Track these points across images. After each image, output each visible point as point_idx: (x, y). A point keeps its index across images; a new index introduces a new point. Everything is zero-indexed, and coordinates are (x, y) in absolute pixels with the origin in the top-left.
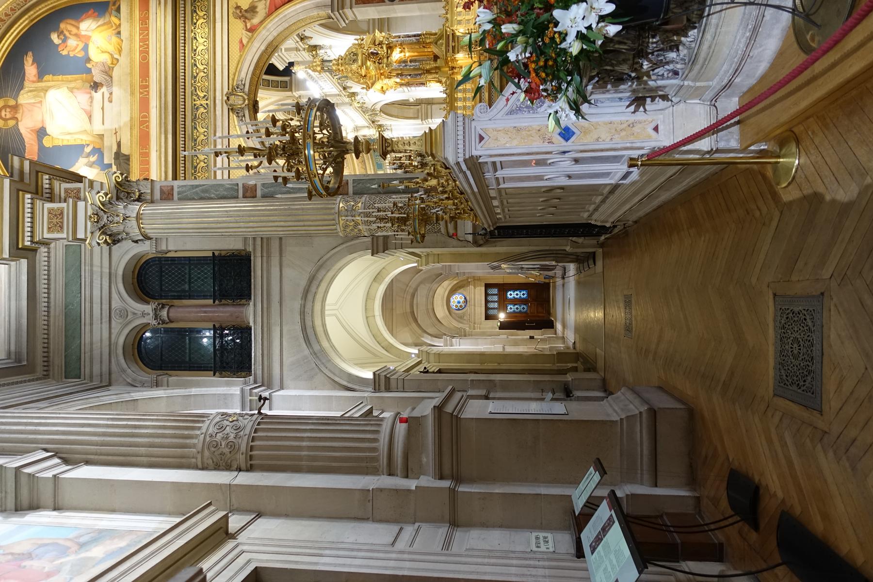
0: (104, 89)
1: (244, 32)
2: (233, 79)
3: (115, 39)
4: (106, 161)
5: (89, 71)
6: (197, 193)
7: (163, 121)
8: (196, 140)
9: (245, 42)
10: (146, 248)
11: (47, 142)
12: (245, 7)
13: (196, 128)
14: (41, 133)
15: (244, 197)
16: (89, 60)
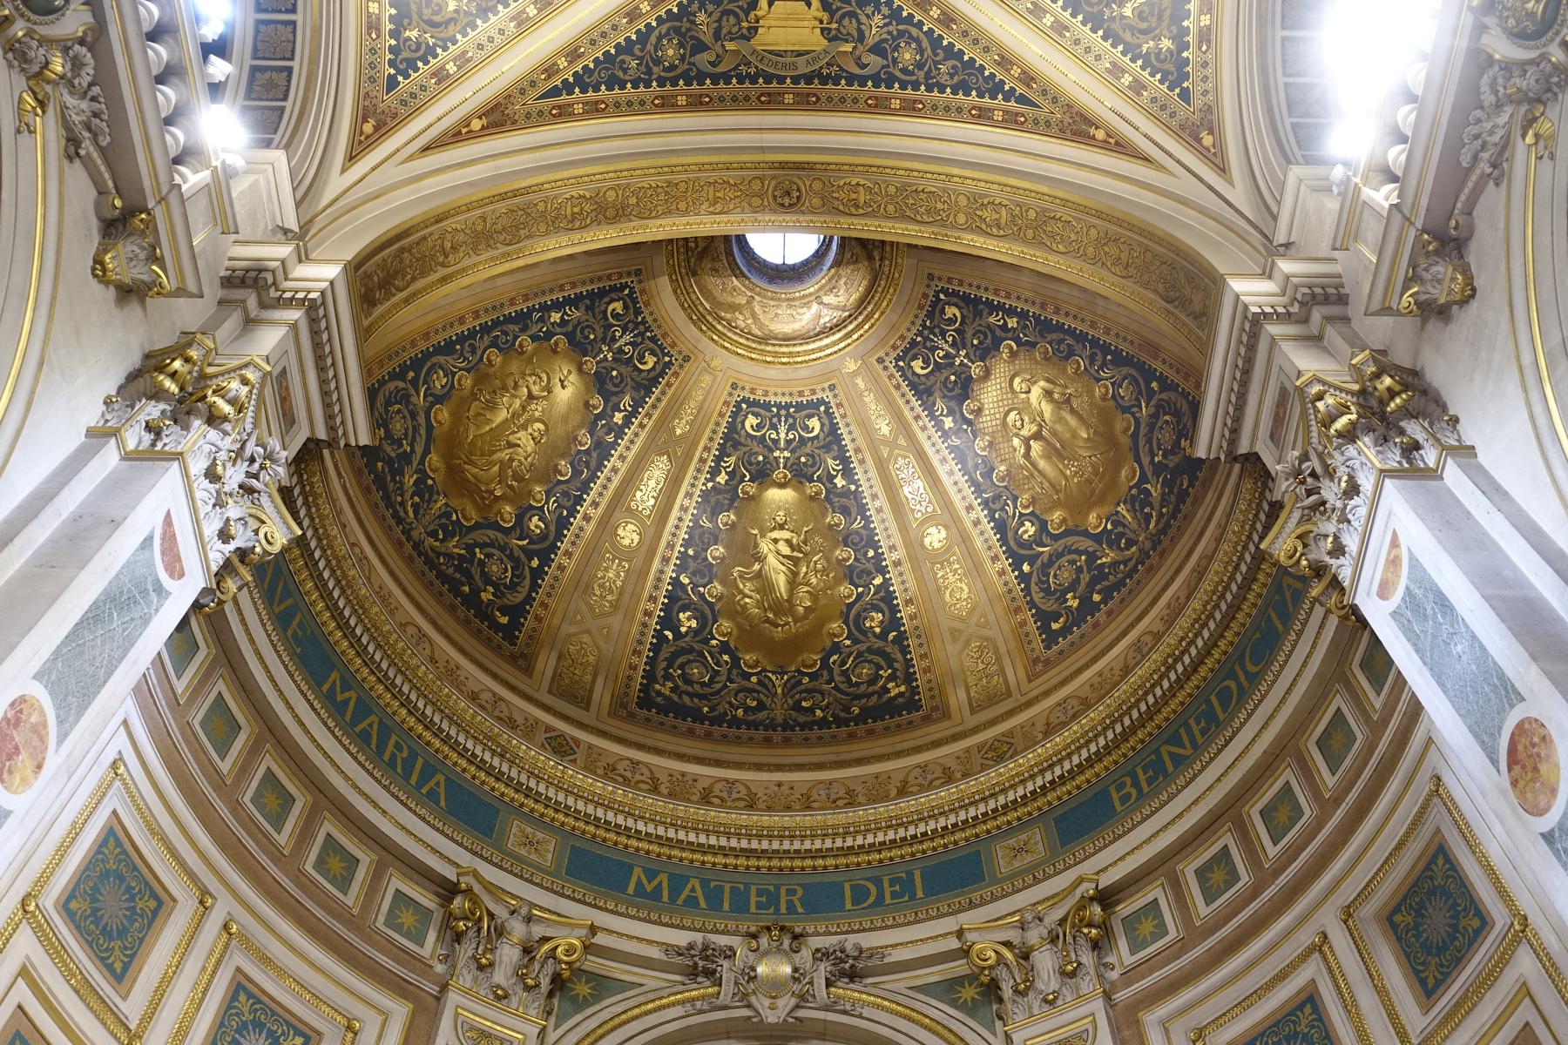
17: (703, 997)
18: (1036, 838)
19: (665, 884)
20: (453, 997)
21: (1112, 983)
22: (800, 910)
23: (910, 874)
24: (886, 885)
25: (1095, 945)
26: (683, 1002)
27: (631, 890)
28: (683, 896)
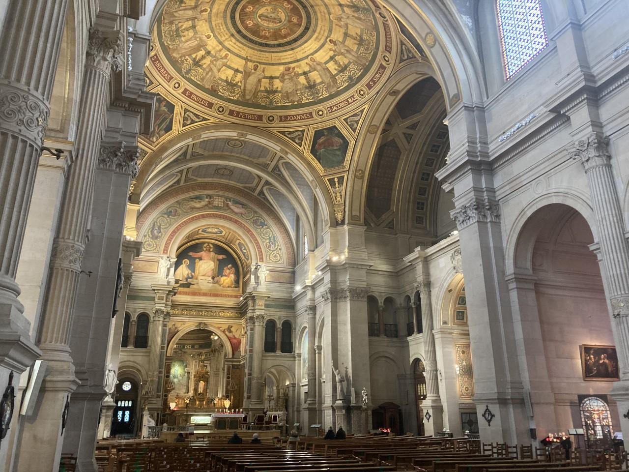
0: (212, 281)
3: (227, 285)
4: (189, 280)
5: (218, 276)
10: (152, 319)
11: (197, 260)
12: (232, 329)
14: (200, 259)
16: (222, 276)
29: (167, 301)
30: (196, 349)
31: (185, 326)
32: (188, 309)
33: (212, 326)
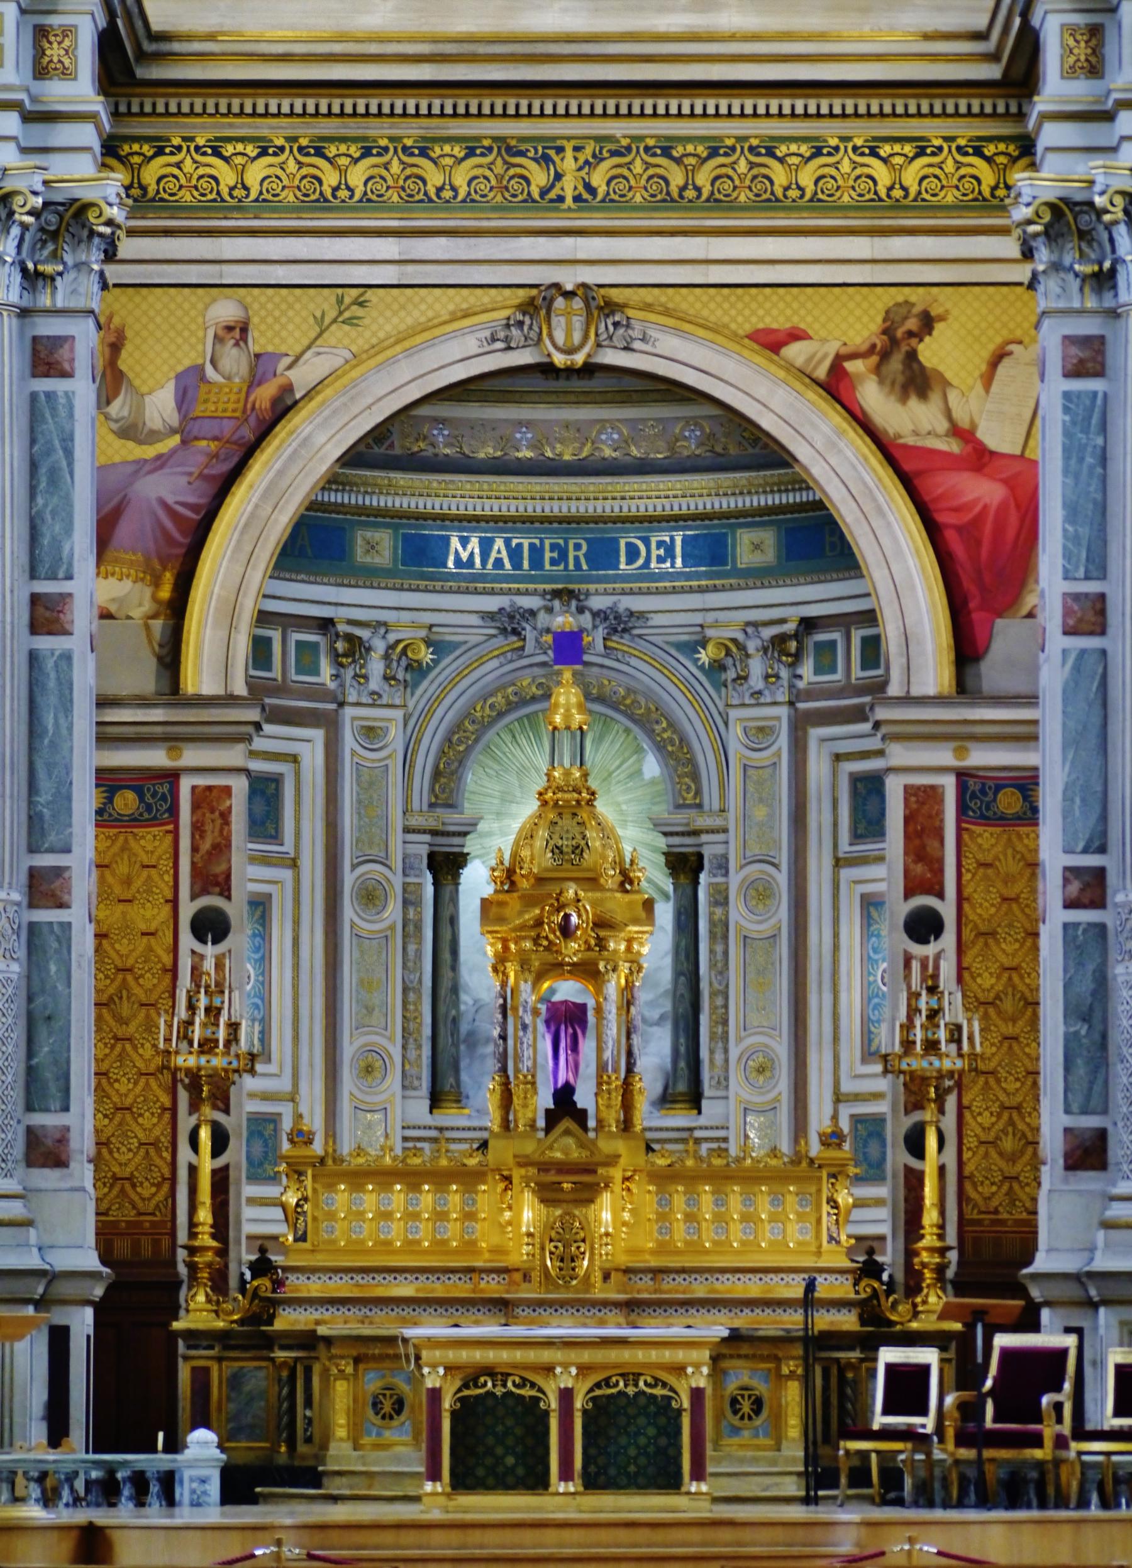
1: (832, 348)
2: (648, 307)
6: (49, 452)
7: (482, 49)
8: (424, 153)
9: (795, 352)
12: (930, 352)
13: (471, 153)
15: (35, 599)
17: (513, 650)
18: (768, 537)
19: (477, 551)
20: (349, 712)
21: (799, 691)
22: (585, 567)
23: (672, 539)
24: (653, 545)
25: (792, 665)
26: (497, 656)
27: (450, 564)
28: (491, 561)
29: (41, 72)
30: (759, 577)
31: (359, 338)
32: (380, 131)
33: (683, 322)
